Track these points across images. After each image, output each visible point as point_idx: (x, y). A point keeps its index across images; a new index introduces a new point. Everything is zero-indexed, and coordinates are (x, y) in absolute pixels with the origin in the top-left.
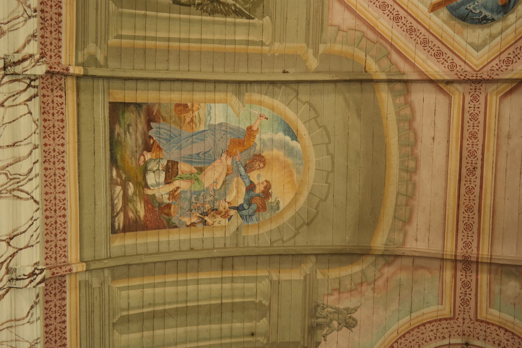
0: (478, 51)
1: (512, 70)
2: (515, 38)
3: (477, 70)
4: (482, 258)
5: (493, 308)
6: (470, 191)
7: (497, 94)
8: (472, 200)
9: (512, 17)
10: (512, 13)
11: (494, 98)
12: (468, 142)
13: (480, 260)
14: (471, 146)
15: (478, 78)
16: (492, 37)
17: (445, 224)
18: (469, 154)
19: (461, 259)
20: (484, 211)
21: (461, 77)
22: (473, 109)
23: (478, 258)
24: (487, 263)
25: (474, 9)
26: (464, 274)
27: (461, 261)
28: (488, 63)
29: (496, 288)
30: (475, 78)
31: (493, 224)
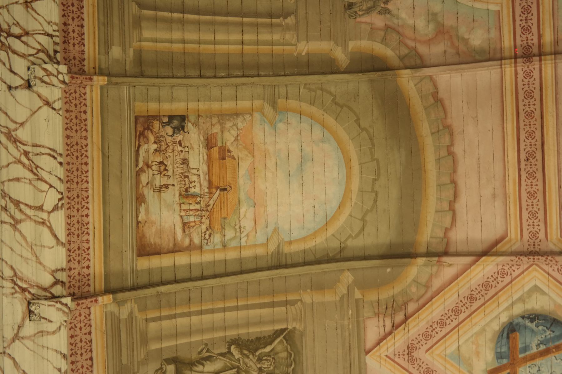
0: (536, 286)
1: (497, 265)
2: (498, 298)
3: (534, 266)
4: (511, 63)
5: (495, 11)
6: (531, 135)
7: (510, 240)
8: (527, 125)
9: (504, 318)
10: (504, 323)
11: (513, 236)
12: (537, 187)
13: (513, 60)
14: (534, 184)
15: (532, 257)
16: (522, 299)
17: (557, 94)
18: (535, 175)
19: (534, 58)
20: (513, 115)
21: (551, 259)
22: (535, 224)
23: (516, 62)
24: (505, 59)
25: (545, 331)
26: (530, 42)
27: (534, 55)
28: (523, 272)
29: (494, 34)
30: (536, 257)
31: (503, 102)
